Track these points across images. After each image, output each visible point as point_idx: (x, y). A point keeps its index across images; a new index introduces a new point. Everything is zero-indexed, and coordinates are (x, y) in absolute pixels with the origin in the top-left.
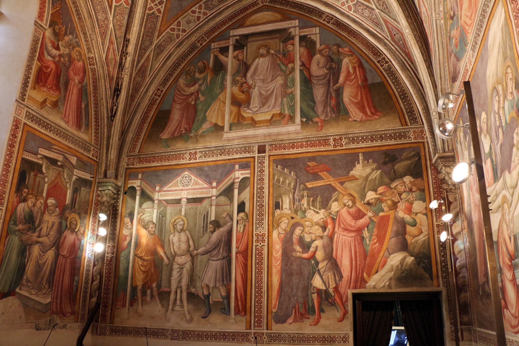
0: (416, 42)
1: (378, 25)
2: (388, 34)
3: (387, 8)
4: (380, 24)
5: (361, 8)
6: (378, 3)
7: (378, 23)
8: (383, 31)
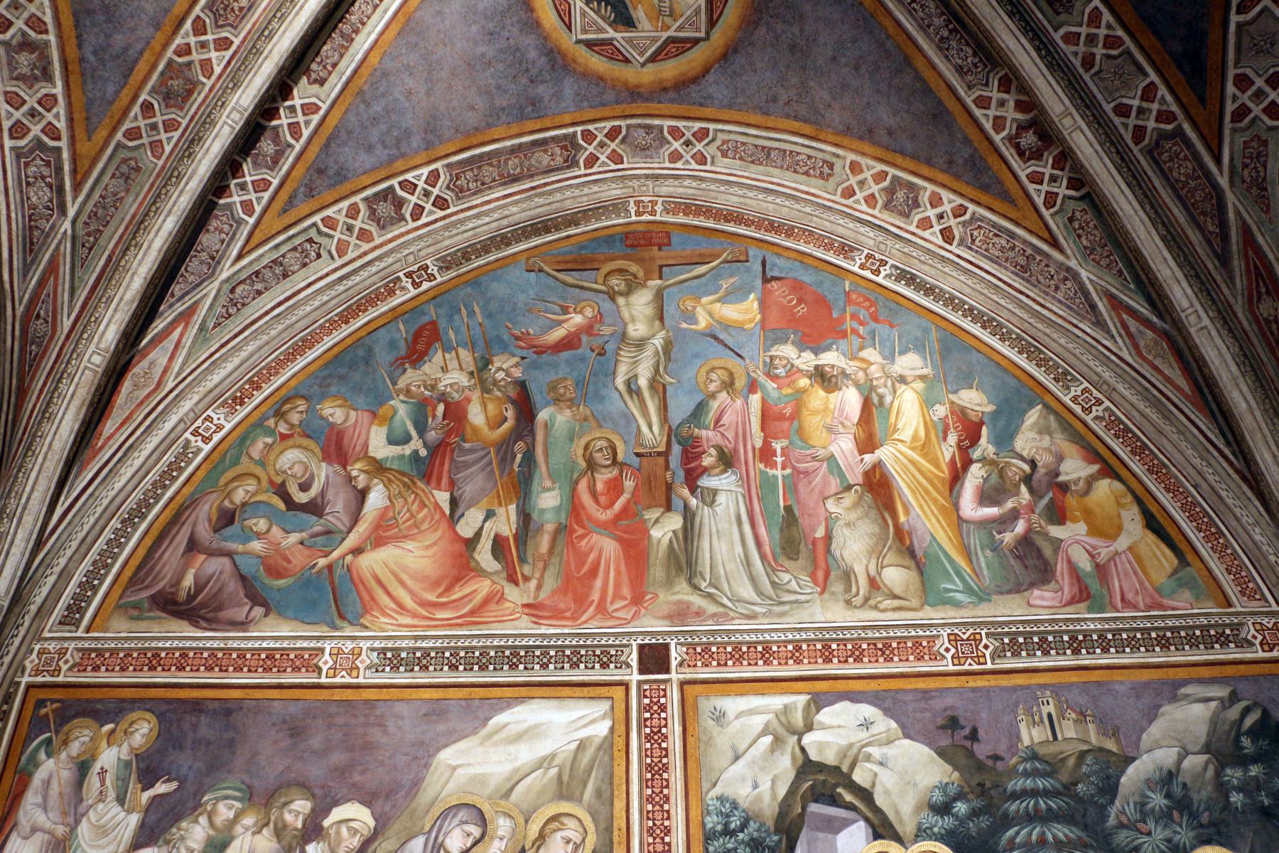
0: (87, 403)
1: (31, 250)
2: (27, 296)
3: (91, 249)
4: (36, 257)
5: (46, 172)
6: (89, 217)
7: (36, 248)
8: (25, 276)
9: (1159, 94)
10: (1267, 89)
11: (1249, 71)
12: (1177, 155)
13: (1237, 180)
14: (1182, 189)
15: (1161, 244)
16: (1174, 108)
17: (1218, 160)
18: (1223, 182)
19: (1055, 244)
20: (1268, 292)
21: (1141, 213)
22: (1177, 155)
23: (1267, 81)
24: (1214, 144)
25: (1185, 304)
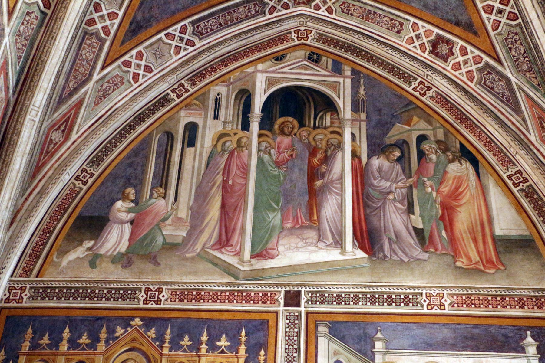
9: (115, 21)
10: (142, 68)
11: (145, 55)
12: (93, 47)
13: (100, 83)
14: (79, 60)
15: (55, 73)
16: (112, 32)
17: (103, 68)
18: (96, 77)
19: (11, 13)
20: (63, 131)
21: (63, 53)
22: (93, 47)
23: (145, 66)
24: (108, 62)
25: (37, 104)
